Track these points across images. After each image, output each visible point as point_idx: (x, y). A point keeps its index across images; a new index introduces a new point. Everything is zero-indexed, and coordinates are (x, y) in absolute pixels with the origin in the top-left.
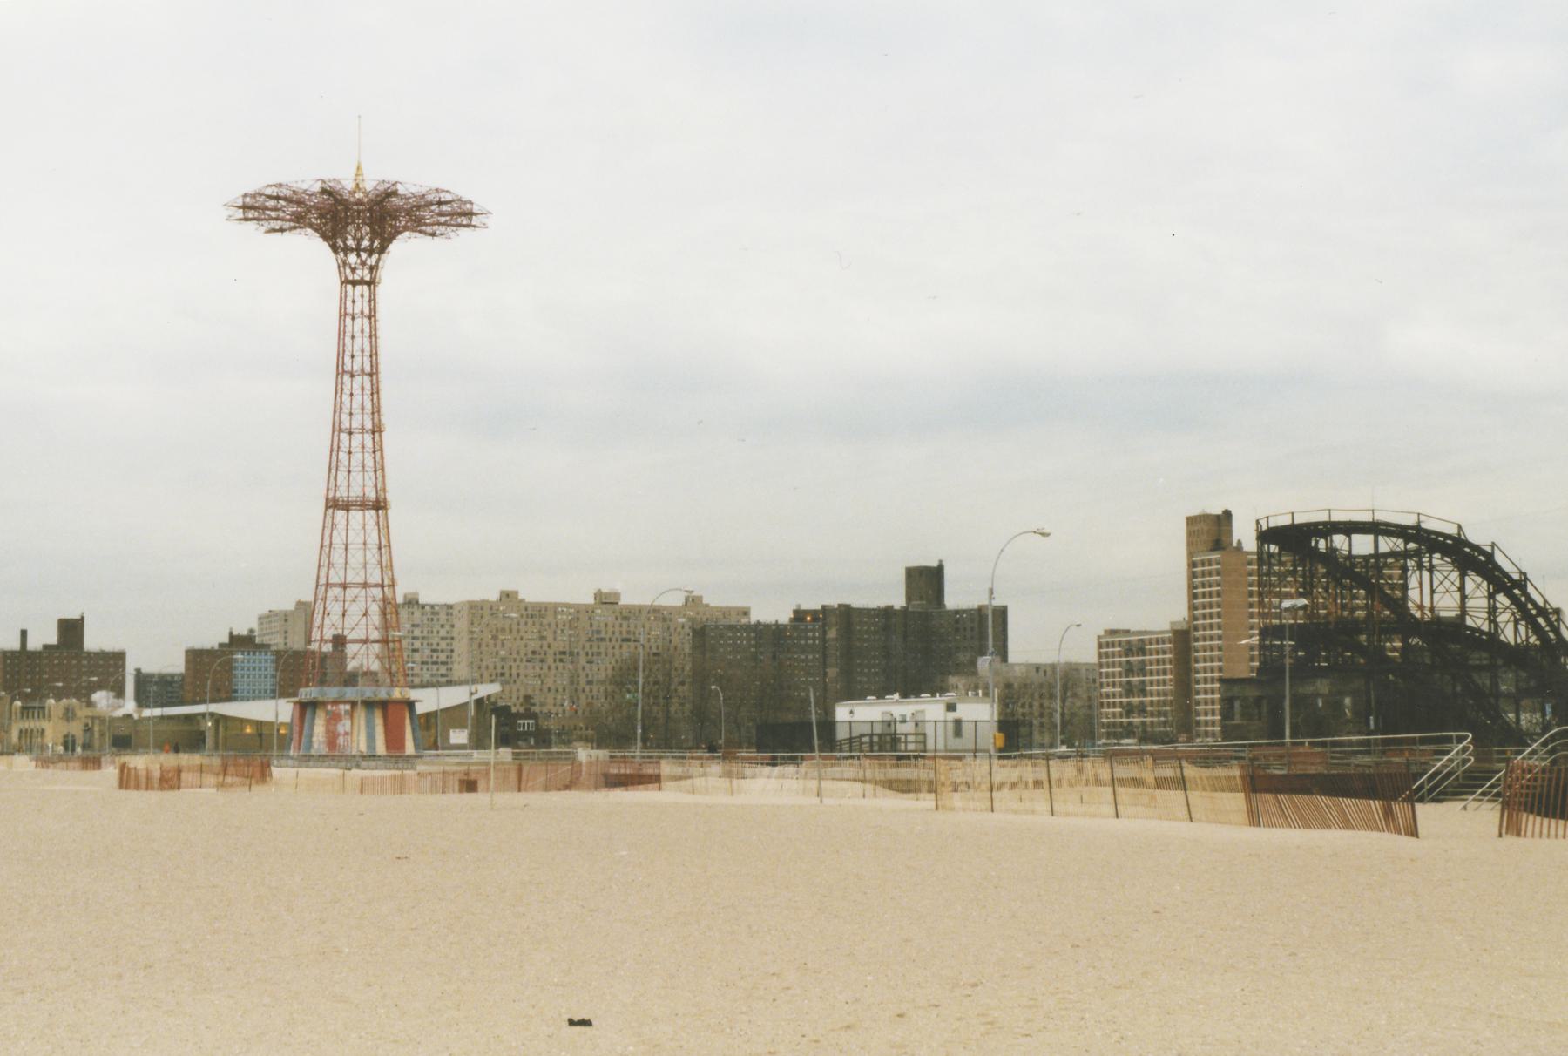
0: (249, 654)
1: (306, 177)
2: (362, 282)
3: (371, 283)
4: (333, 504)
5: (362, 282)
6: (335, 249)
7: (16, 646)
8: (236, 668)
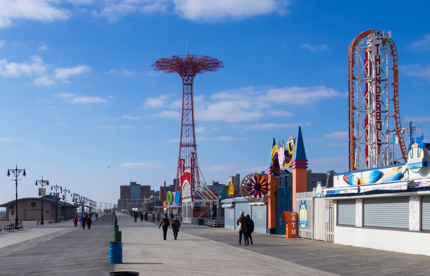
0: (217, 187)
1: (169, 55)
2: (189, 84)
3: (191, 85)
4: (181, 145)
5: (189, 84)
7: (164, 186)
8: (131, 192)
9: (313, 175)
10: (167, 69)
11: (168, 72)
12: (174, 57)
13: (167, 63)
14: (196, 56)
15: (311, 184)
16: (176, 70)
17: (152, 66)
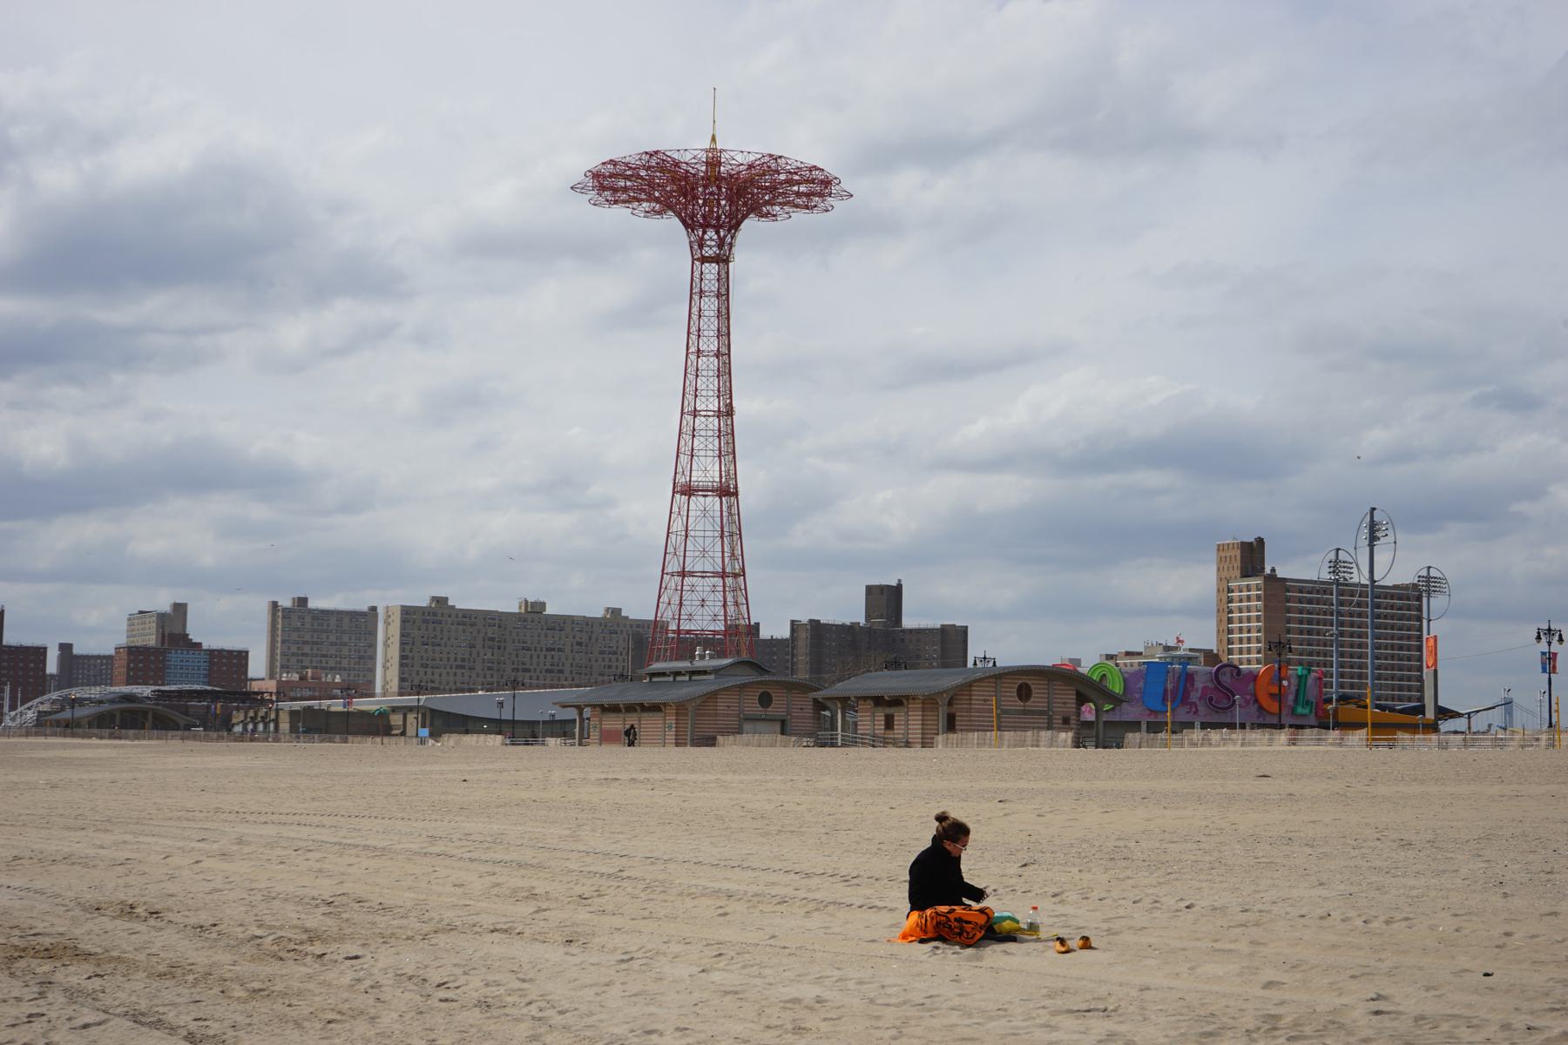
3: (723, 260)
6: (689, 224)
9: (638, 626)
10: (638, 200)
11: (648, 212)
12: (651, 155)
13: (627, 178)
14: (732, 154)
15: (542, 658)
16: (670, 207)
17: (578, 190)
